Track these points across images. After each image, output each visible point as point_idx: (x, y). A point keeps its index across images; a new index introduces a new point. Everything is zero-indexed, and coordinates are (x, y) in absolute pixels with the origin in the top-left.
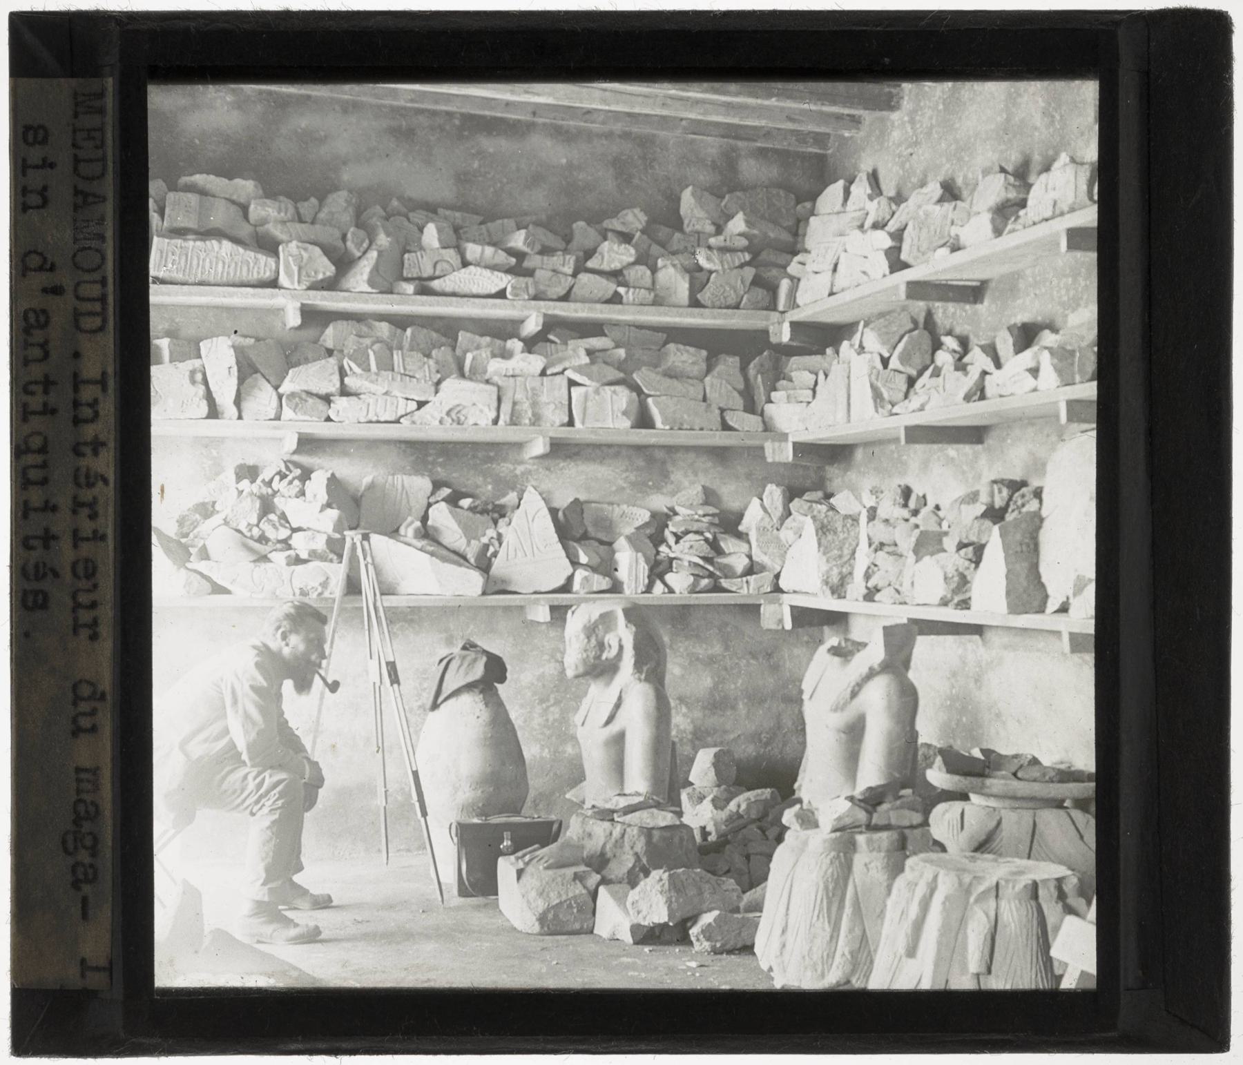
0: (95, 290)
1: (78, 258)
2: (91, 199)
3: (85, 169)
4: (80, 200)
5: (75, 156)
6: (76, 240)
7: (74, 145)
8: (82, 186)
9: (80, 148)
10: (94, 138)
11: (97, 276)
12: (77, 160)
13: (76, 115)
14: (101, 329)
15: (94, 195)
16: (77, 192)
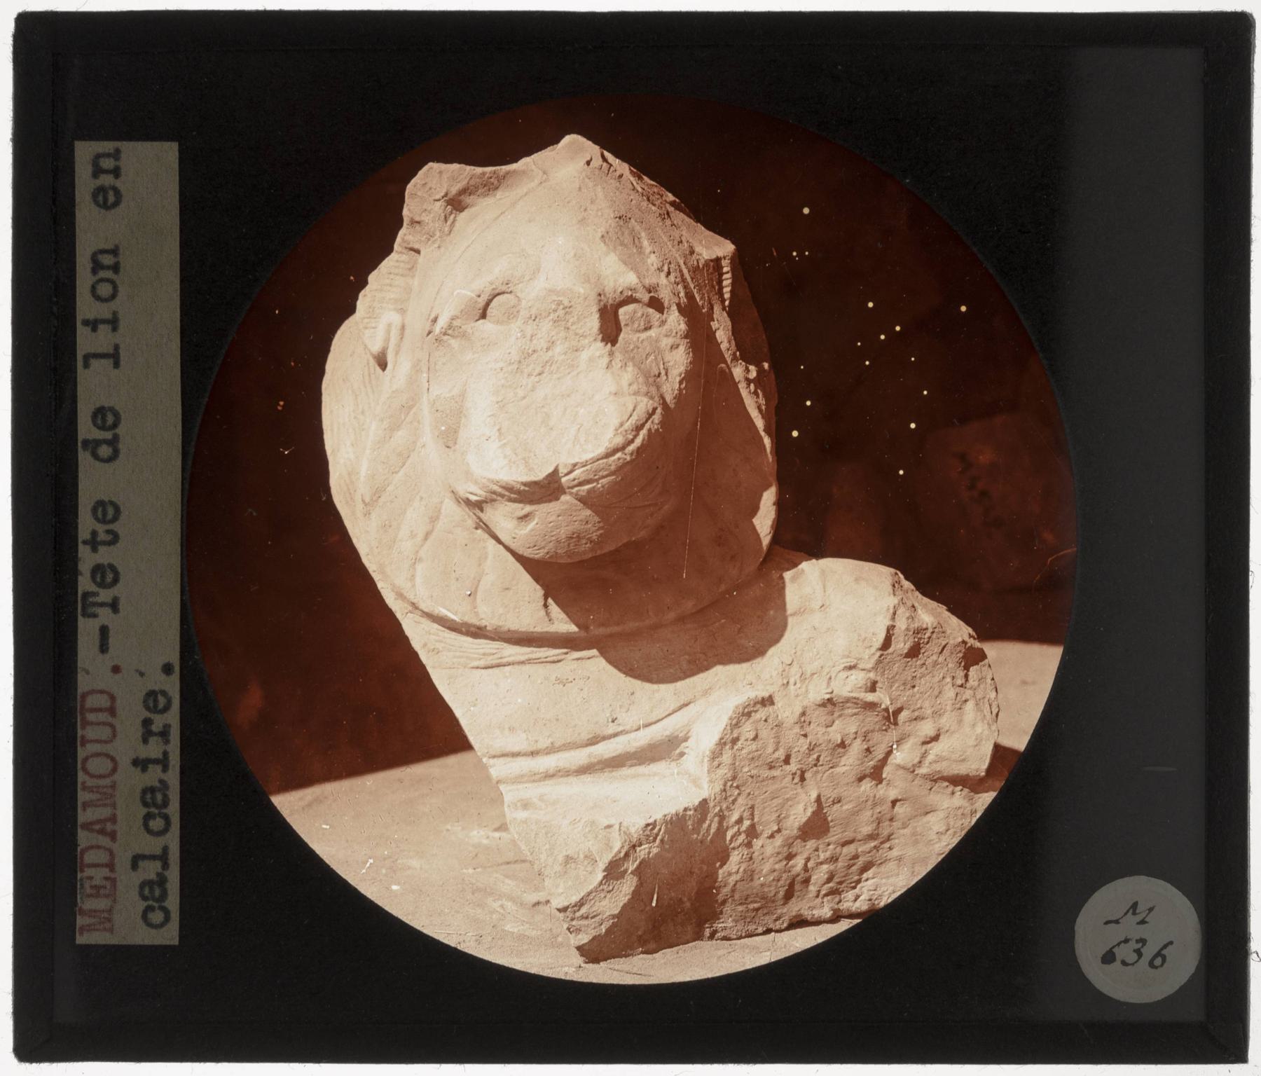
0: (90, 733)
1: (110, 765)
2: (97, 827)
3: (102, 857)
4: (109, 827)
5: (112, 869)
6: (113, 786)
7: (114, 881)
8: (104, 841)
9: (106, 878)
10: (92, 887)
11: (92, 748)
12: (111, 866)
13: (110, 911)
14: (84, 696)
15: (92, 831)
16: (113, 836)
